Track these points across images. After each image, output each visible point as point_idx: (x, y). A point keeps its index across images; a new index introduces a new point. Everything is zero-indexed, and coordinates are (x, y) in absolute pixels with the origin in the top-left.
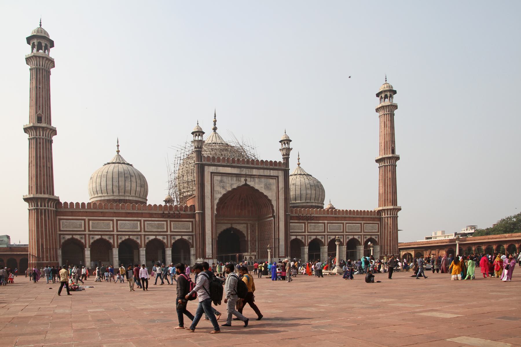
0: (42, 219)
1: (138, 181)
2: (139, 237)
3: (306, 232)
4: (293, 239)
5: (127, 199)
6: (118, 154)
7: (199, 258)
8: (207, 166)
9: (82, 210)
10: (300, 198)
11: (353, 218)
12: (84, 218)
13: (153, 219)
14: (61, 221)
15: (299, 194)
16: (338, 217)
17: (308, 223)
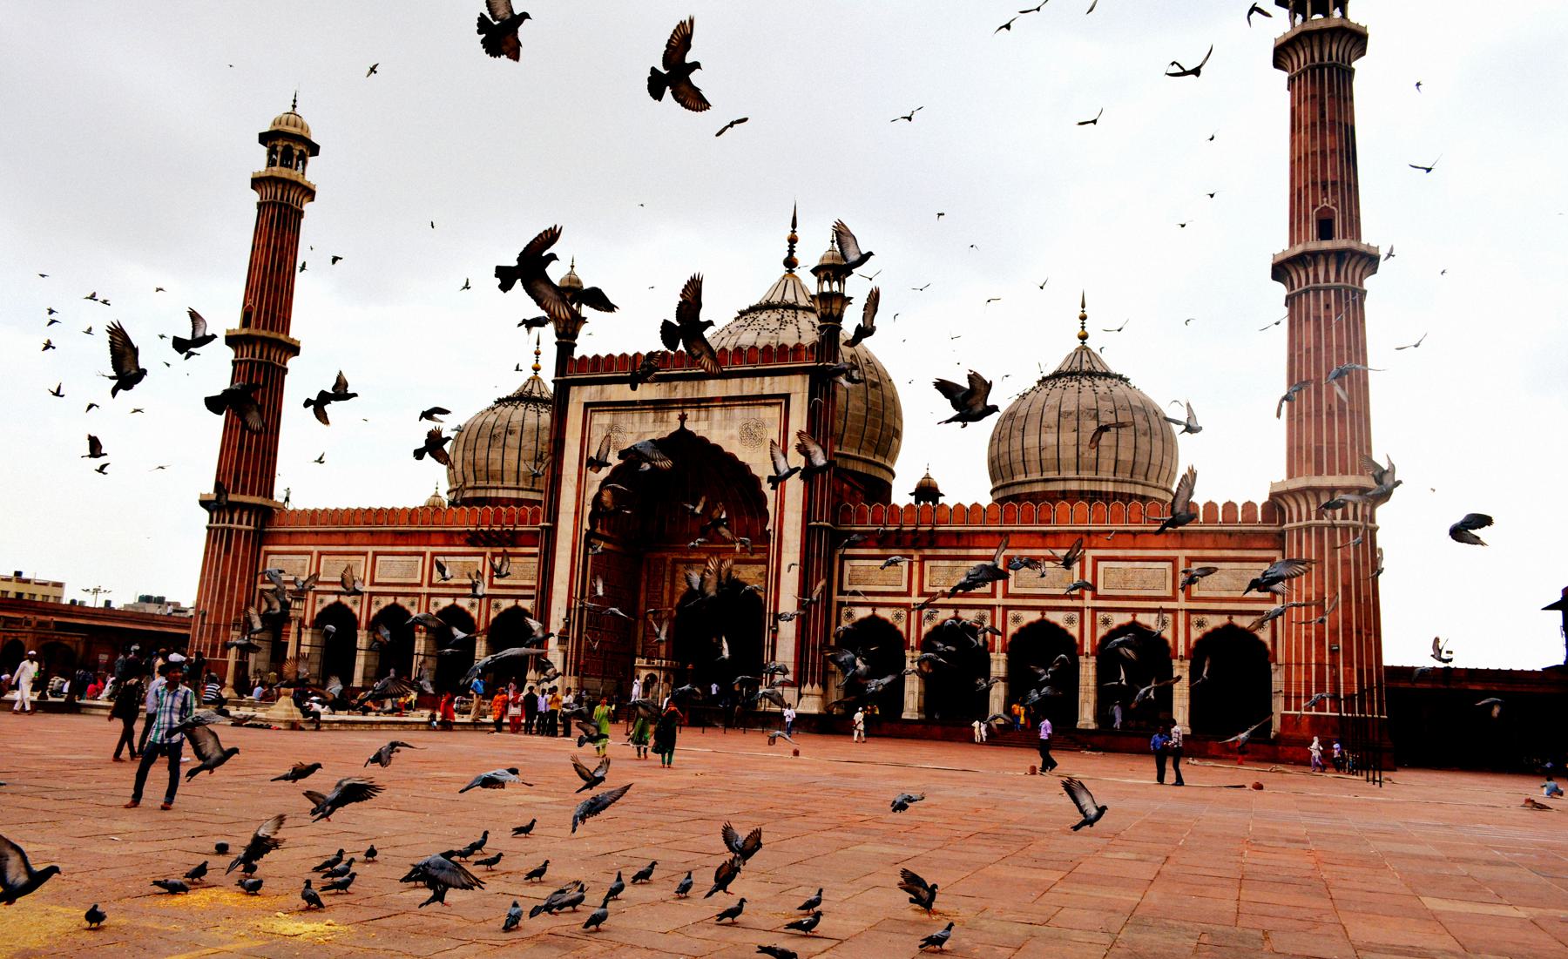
0: (213, 553)
1: (529, 445)
2: (417, 599)
3: (915, 591)
4: (862, 620)
5: (493, 495)
6: (536, 374)
7: (533, 670)
8: (577, 387)
9: (307, 529)
10: (1022, 464)
11: (1131, 536)
12: (311, 548)
13: (453, 549)
14: (270, 557)
15: (1017, 451)
16: (1055, 534)
17: (923, 559)
